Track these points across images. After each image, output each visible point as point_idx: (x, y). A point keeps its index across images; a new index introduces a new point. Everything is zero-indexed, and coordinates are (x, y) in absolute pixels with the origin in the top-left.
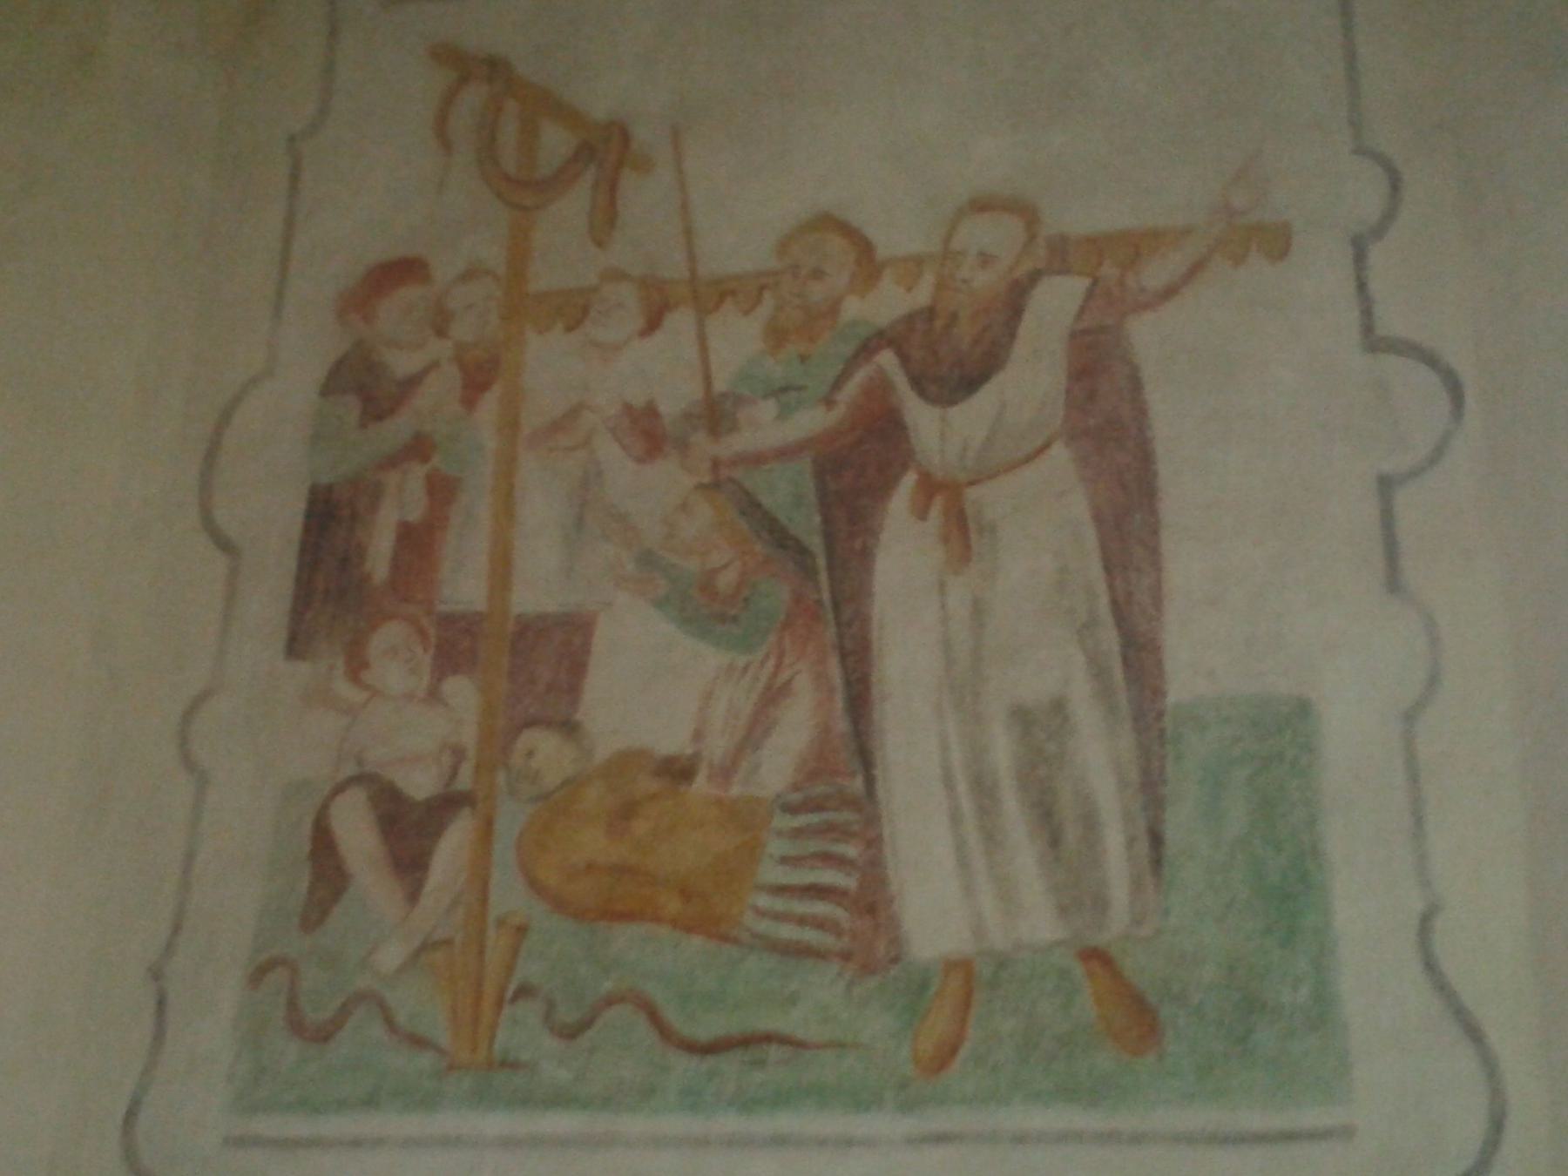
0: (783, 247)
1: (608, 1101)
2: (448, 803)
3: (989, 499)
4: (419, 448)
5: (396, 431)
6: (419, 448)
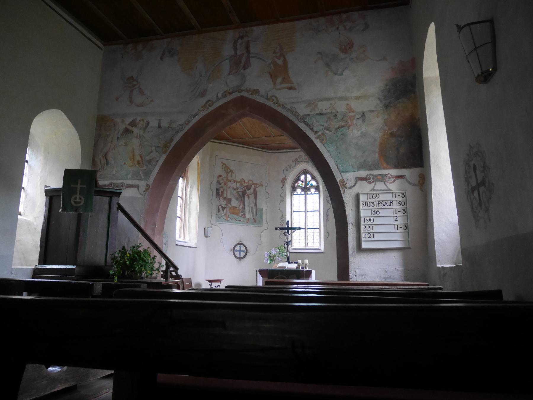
0: (241, 180)
1: (233, 223)
2: (225, 207)
3: (250, 196)
4: (222, 187)
5: (221, 186)
6: (222, 187)
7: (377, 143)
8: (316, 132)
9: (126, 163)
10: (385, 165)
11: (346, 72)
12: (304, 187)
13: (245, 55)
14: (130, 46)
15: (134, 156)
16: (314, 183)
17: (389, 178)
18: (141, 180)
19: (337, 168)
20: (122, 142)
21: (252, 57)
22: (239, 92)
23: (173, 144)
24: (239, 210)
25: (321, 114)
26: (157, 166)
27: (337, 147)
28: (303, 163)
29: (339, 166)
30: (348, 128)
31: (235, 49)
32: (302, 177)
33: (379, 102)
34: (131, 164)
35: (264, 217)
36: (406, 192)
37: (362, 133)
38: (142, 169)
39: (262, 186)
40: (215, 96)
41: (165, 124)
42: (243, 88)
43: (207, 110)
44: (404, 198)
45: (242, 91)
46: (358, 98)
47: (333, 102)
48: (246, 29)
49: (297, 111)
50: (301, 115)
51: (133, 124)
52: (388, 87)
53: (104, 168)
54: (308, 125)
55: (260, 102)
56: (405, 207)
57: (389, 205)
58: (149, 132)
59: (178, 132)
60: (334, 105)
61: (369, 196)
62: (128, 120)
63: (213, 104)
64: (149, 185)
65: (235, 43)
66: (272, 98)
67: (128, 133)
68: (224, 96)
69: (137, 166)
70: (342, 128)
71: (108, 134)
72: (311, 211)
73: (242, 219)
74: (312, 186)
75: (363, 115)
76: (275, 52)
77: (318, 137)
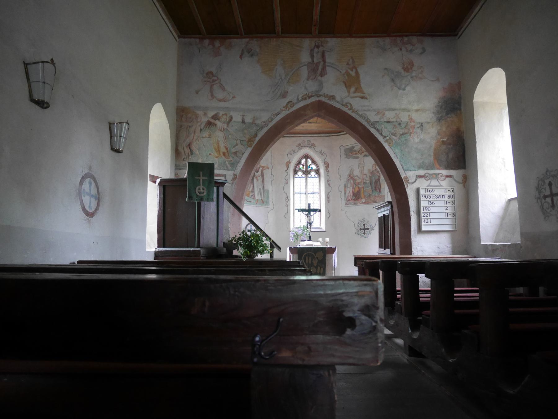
3: (258, 178)
7: (433, 148)
8: (385, 137)
9: (212, 154)
10: (438, 166)
11: (408, 88)
12: (304, 170)
13: (322, 63)
14: (206, 42)
15: (219, 147)
16: (314, 167)
17: (441, 177)
18: (228, 170)
19: (401, 167)
20: (206, 134)
21: (328, 66)
22: (317, 97)
23: (257, 139)
24: (249, 191)
25: (388, 122)
26: (243, 158)
27: (401, 150)
28: (306, 148)
29: (403, 165)
30: (410, 135)
31: (312, 56)
32: (303, 161)
33: (433, 115)
34: (217, 155)
35: (270, 199)
36: (454, 188)
37: (421, 140)
38: (227, 159)
39: (269, 168)
40: (296, 98)
41: (248, 120)
42: (321, 93)
43: (288, 110)
44: (453, 193)
45: (320, 96)
46: (417, 111)
47: (397, 112)
48: (321, 39)
49: (368, 118)
50: (372, 120)
51: (215, 117)
52: (440, 104)
53: (188, 157)
54: (378, 130)
55: (337, 107)
56: (453, 199)
57: (442, 197)
58: (232, 126)
59: (262, 128)
60: (399, 115)
61: (426, 190)
62: (211, 114)
63: (294, 105)
64: (237, 176)
65: (312, 51)
66: (347, 104)
67: (211, 126)
68: (304, 99)
69: (223, 157)
70: (406, 135)
71: (190, 124)
72: (312, 193)
73: (252, 200)
74: (312, 170)
75: (422, 125)
76: (348, 64)
77: (386, 141)
